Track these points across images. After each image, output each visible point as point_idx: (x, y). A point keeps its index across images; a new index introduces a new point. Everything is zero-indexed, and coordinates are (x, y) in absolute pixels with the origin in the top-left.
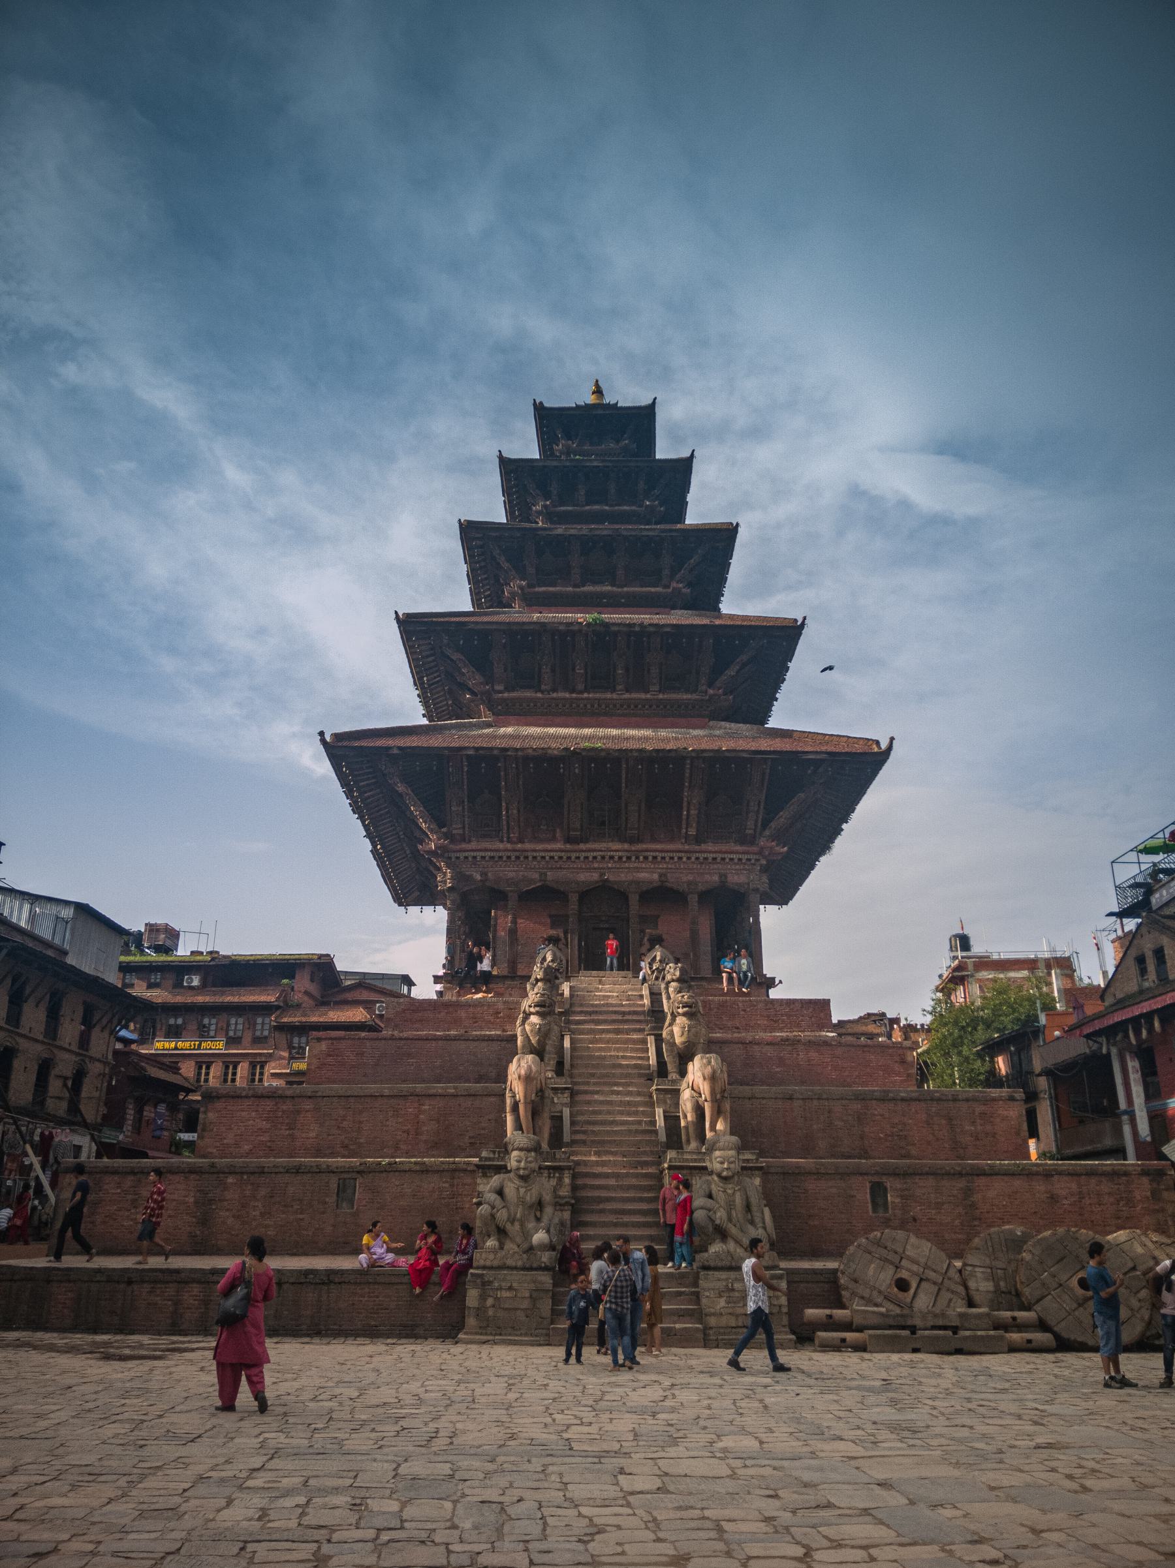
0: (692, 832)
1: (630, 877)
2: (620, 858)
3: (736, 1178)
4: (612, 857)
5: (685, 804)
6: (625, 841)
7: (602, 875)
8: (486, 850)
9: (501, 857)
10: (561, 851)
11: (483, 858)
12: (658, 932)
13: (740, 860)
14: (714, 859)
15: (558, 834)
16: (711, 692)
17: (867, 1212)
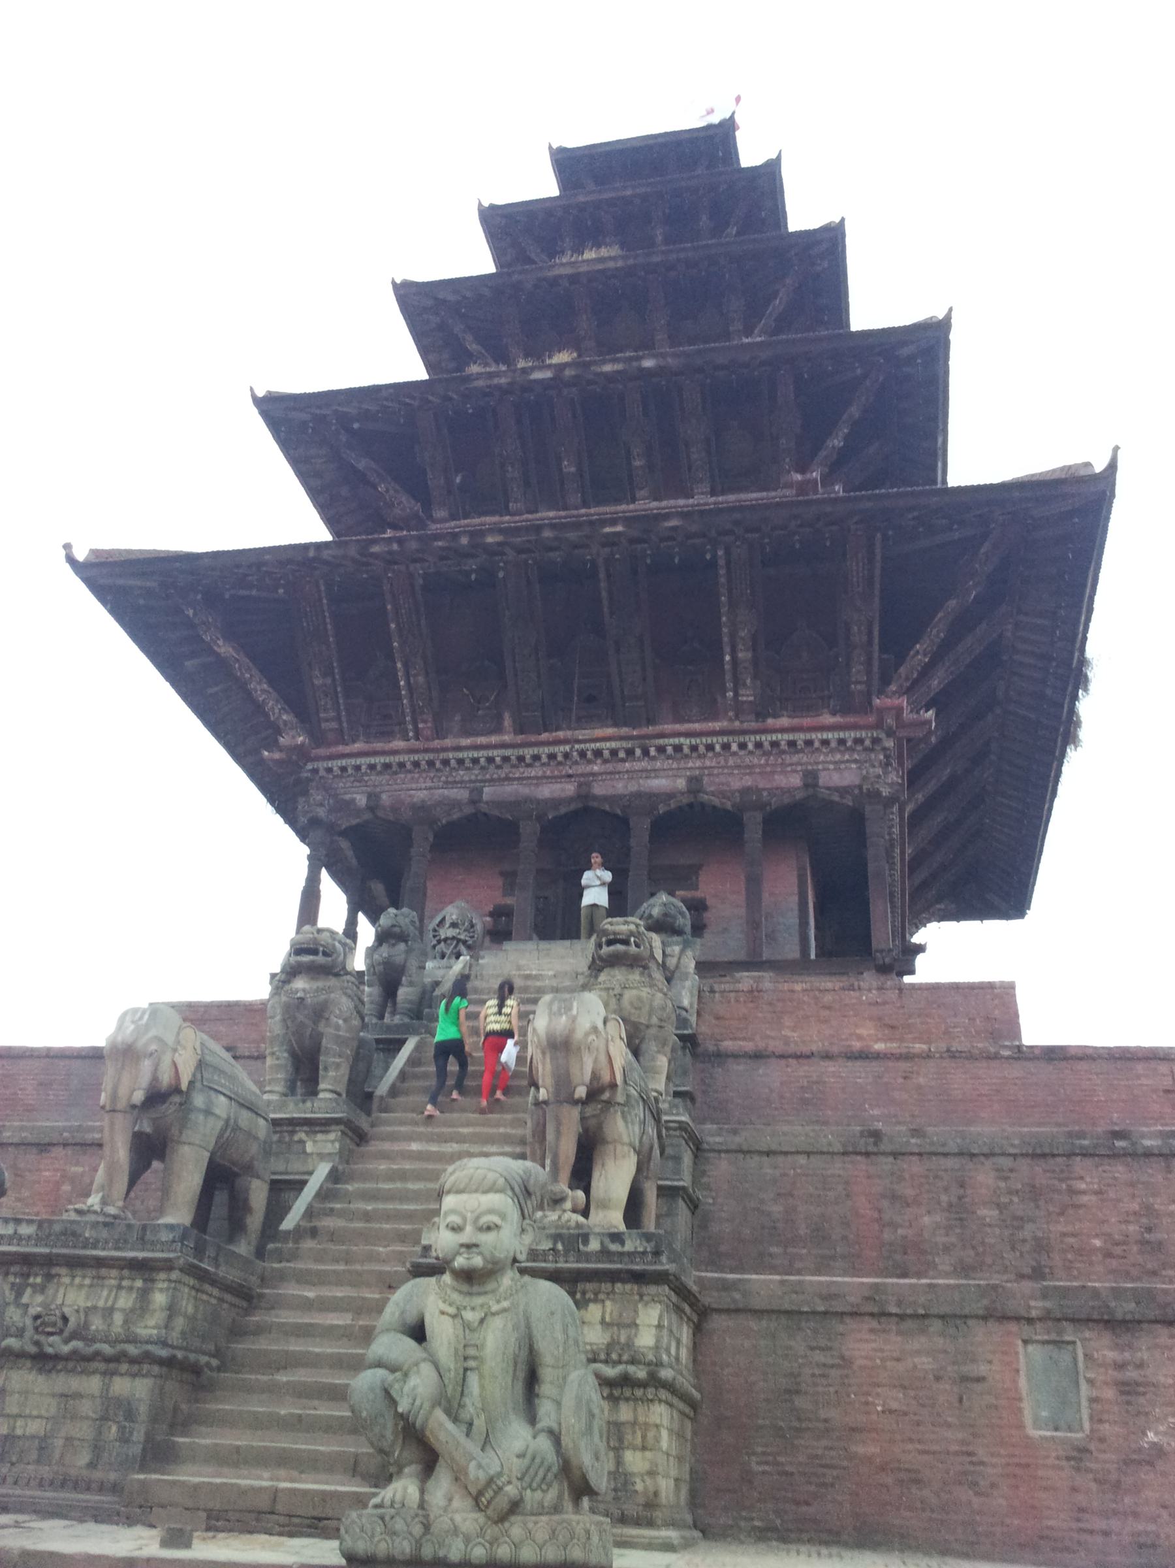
0: (747, 696)
1: (633, 787)
2: (614, 752)
3: (508, 1279)
4: (598, 753)
5: (726, 639)
6: (625, 725)
7: (580, 785)
8: (375, 753)
9: (402, 765)
10: (503, 746)
11: (372, 767)
12: (698, 894)
13: (842, 742)
14: (792, 744)
15: (507, 722)
16: (799, 477)
17: (1021, 1426)
